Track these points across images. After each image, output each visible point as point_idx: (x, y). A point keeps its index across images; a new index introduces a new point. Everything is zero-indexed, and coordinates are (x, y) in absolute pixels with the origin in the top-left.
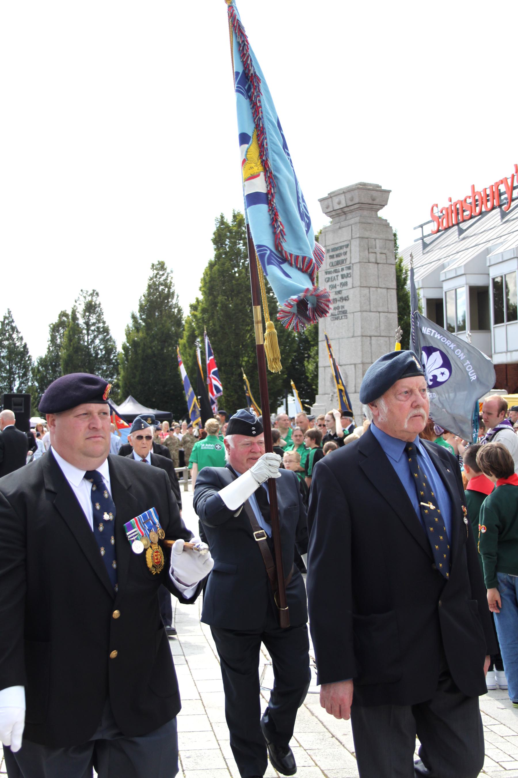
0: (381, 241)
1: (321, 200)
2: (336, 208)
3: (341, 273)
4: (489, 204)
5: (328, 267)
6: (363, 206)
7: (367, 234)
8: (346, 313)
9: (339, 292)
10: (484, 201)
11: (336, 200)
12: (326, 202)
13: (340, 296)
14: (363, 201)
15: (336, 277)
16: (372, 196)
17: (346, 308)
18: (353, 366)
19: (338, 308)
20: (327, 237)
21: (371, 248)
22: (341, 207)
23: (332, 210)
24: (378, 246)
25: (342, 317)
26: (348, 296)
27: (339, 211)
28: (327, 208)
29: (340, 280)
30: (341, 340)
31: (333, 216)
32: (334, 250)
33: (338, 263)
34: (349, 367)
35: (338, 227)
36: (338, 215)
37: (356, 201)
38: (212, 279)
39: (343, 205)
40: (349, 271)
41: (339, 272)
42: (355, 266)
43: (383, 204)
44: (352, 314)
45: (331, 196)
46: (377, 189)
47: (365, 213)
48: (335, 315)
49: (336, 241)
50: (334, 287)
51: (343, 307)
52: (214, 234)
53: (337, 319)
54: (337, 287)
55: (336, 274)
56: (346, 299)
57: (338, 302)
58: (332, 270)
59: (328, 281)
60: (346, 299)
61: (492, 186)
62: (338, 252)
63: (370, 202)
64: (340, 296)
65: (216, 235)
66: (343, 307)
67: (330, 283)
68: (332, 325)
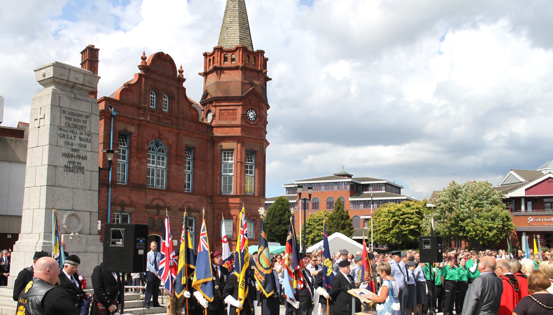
5: (63, 125)
9: (75, 150)
15: (73, 137)
17: (82, 165)
18: (89, 213)
19: (74, 163)
20: (62, 99)
25: (77, 171)
26: (85, 157)
29: (77, 141)
33: (76, 126)
34: (85, 213)
39: (81, 81)
40: (89, 138)
42: (94, 135)
44: (90, 173)
55: (73, 135)
57: (73, 158)
62: (76, 118)
67: (63, 139)
68: (65, 175)
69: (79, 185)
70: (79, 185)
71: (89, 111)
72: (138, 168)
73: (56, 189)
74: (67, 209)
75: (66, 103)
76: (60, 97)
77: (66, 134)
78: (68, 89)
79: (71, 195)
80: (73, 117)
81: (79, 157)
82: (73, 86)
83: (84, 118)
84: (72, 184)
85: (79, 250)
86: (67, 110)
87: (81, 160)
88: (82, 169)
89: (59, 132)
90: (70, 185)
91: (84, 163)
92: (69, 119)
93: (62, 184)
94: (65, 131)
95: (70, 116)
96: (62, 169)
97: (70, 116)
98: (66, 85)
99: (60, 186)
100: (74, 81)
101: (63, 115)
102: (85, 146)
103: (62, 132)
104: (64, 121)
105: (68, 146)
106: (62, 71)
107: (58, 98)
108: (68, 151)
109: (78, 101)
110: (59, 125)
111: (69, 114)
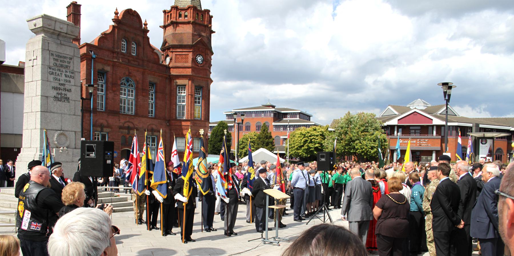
2: (57, 29)
5: (52, 65)
9: (62, 84)
17: (68, 96)
19: (61, 94)
29: (63, 78)
39: (65, 30)
40: (72, 75)
42: (76, 73)
51: (65, 95)
55: (60, 73)
56: (69, 91)
57: (61, 91)
60: (69, 91)
62: (62, 59)
67: (52, 76)
69: (66, 111)
70: (66, 111)
71: (72, 54)
72: (113, 99)
73: (48, 114)
74: (57, 129)
75: (53, 47)
76: (48, 43)
78: (55, 37)
79: (60, 119)
80: (59, 59)
81: (65, 90)
82: (59, 34)
83: (68, 60)
85: (68, 160)
86: (54, 53)
87: (67, 92)
88: (68, 99)
89: (49, 70)
90: (59, 111)
91: (69, 95)
92: (57, 60)
93: (52, 110)
94: (53, 69)
95: (57, 58)
96: (52, 99)
97: (57, 58)
98: (53, 33)
99: (51, 112)
100: (60, 30)
101: (51, 57)
102: (70, 82)
103: (51, 70)
104: (52, 62)
106: (49, 22)
107: (47, 44)
108: (56, 85)
109: (63, 46)
110: (48, 65)
111: (56, 56)
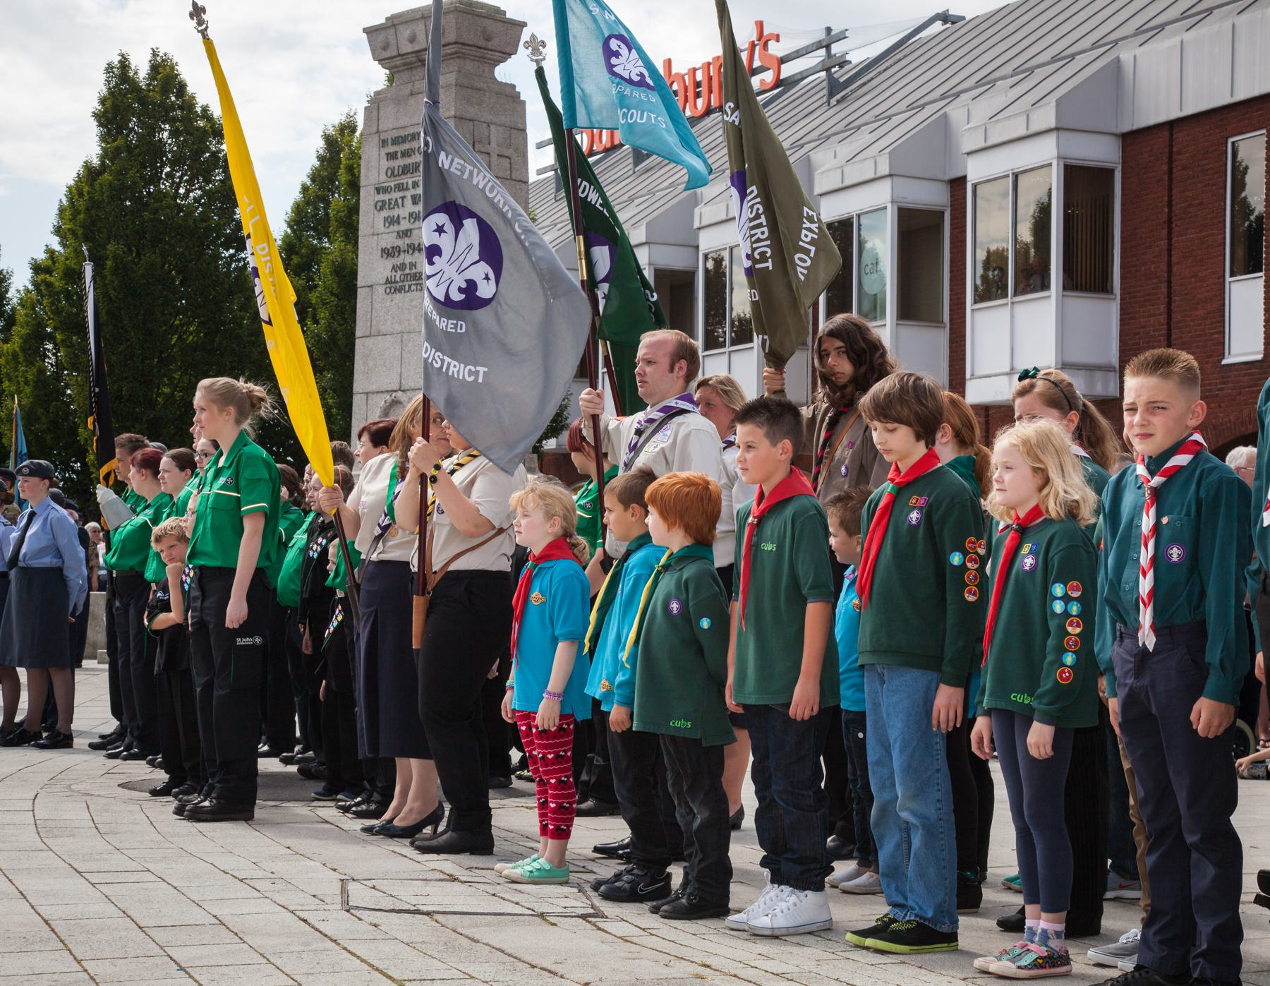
0: (501, 129)
1: (370, 31)
2: (403, 51)
3: (413, 192)
4: (700, 103)
5: (383, 177)
6: (465, 50)
7: (472, 111)
8: (420, 278)
9: (406, 233)
10: (691, 94)
11: (405, 33)
12: (381, 37)
13: (408, 241)
14: (465, 39)
16: (484, 30)
19: (402, 267)
21: (480, 142)
22: (417, 48)
23: (395, 53)
24: (493, 139)
27: (412, 59)
28: (385, 48)
30: (406, 336)
31: (396, 67)
32: (396, 141)
35: (407, 92)
36: (409, 67)
37: (451, 37)
38: (94, 205)
41: (407, 189)
43: (508, 51)
45: (394, 22)
46: (496, 15)
47: (469, 66)
48: (396, 282)
49: (402, 123)
50: (397, 221)
52: (103, 101)
53: (400, 290)
54: (402, 222)
55: (401, 194)
58: (392, 184)
59: (381, 209)
61: (709, 64)
62: (406, 146)
63: (481, 43)
64: (408, 241)
65: (108, 104)
66: (413, 265)
67: (385, 213)
69: (413, 321)
70: (413, 321)
77: (386, 197)
84: (400, 323)
93: (384, 329)
96: (381, 290)
99: (379, 334)
101: (384, 151)
104: (385, 164)
105: (392, 228)
